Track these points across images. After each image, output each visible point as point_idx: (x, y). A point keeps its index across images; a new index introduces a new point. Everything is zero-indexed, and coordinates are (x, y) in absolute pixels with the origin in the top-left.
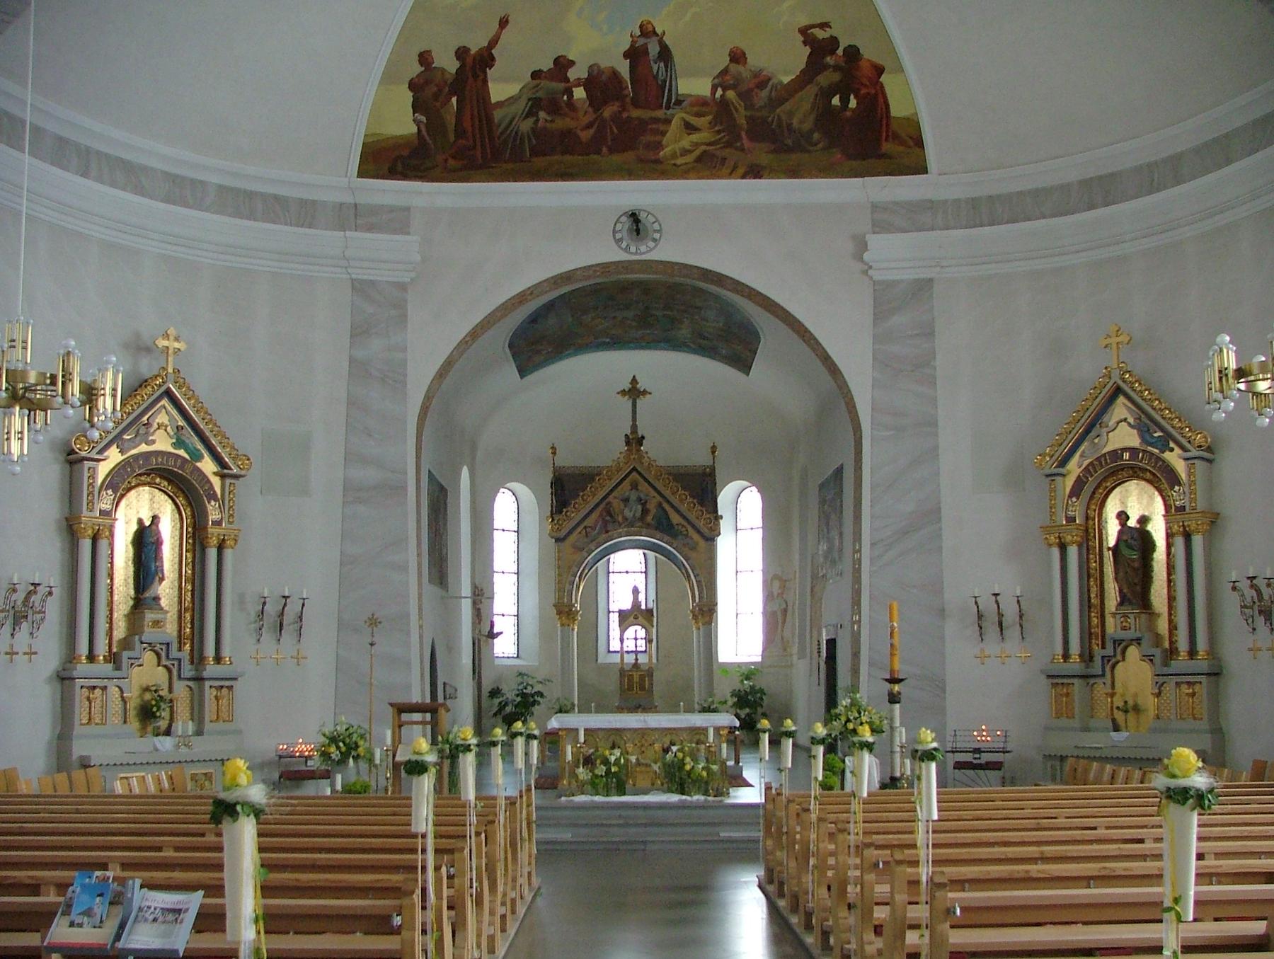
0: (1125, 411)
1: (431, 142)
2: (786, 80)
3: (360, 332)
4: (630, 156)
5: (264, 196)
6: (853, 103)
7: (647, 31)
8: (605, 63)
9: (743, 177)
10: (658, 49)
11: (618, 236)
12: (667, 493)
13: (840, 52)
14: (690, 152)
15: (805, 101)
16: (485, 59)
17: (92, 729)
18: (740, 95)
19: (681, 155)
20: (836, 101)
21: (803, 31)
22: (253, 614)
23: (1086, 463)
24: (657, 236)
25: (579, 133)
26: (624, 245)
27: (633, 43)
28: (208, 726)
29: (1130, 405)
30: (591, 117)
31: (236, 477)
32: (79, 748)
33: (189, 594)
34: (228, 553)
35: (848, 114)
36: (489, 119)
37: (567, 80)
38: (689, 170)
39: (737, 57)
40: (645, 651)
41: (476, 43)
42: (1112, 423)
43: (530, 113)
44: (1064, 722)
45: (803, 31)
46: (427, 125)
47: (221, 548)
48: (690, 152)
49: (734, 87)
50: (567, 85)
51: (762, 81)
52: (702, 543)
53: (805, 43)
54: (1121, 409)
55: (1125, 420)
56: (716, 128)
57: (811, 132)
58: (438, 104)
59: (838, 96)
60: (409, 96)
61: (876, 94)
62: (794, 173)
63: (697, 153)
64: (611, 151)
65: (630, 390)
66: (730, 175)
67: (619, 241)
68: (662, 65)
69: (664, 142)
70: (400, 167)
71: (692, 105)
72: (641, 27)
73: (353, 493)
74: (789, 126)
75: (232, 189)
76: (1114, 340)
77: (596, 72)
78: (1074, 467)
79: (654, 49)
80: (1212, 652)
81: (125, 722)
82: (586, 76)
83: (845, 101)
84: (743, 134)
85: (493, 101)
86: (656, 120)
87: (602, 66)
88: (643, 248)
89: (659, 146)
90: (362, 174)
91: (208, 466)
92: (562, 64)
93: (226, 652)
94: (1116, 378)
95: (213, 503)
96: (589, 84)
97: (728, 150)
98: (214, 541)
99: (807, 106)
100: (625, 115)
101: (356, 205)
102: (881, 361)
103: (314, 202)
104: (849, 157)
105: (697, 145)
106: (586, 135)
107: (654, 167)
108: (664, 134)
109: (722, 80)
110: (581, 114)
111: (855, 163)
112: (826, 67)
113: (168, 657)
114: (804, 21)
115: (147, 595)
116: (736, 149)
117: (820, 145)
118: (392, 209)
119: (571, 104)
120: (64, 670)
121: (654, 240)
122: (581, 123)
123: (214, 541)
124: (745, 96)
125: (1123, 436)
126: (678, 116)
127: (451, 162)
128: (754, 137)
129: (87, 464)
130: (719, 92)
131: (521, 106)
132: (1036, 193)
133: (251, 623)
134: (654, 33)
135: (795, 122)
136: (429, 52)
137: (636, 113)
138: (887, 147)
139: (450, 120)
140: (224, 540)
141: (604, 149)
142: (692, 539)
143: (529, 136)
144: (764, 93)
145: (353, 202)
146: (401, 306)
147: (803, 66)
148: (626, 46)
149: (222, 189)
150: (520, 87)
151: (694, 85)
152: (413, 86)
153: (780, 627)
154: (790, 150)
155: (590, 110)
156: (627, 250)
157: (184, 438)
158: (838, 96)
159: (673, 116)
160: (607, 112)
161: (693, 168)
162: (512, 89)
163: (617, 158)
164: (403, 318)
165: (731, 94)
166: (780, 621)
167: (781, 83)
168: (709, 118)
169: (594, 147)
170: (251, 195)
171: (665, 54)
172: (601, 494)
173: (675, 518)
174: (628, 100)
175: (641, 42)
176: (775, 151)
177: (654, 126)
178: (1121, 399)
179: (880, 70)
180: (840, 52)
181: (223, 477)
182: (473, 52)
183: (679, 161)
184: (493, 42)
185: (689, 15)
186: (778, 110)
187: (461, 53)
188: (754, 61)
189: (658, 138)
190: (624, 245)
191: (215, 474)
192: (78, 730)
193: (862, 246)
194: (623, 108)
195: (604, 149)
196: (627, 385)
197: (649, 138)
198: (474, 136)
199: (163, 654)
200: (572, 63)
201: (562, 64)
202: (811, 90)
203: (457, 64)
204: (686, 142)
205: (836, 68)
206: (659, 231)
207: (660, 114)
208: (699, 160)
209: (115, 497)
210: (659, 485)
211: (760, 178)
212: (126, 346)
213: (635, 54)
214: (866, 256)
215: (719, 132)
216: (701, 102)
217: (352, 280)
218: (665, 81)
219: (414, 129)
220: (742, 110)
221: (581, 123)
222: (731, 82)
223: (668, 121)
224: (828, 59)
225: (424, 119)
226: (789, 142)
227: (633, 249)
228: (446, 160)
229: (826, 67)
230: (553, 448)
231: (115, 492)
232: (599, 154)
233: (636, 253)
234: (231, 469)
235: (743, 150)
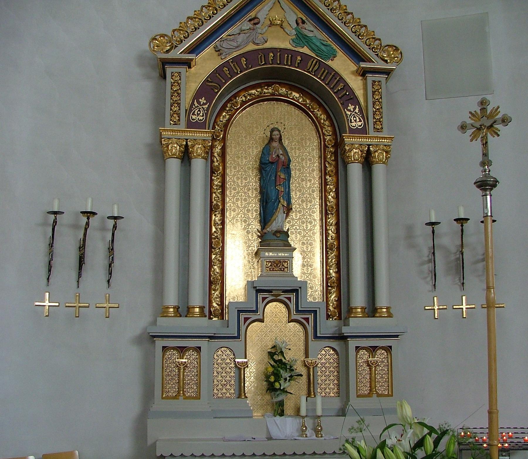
17: (180, 404)
22: (426, 252)
28: (354, 402)
33: (333, 228)
34: (379, 170)
81: (239, 396)
93: (382, 301)
95: (351, 107)
98: (355, 153)
123: (355, 153)
133: (422, 264)
140: (369, 152)
157: (306, 32)
181: (363, 73)
209: (209, 106)
231: (209, 100)
234: (370, 61)
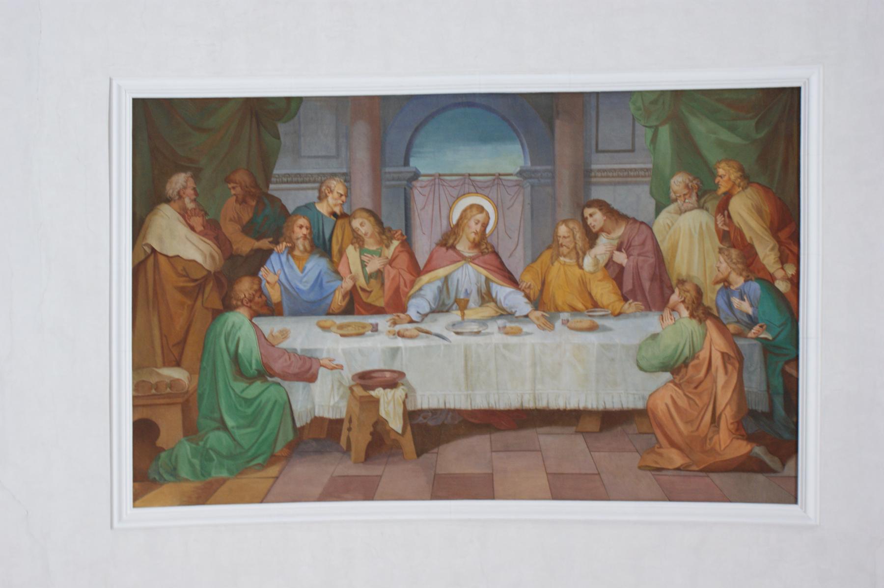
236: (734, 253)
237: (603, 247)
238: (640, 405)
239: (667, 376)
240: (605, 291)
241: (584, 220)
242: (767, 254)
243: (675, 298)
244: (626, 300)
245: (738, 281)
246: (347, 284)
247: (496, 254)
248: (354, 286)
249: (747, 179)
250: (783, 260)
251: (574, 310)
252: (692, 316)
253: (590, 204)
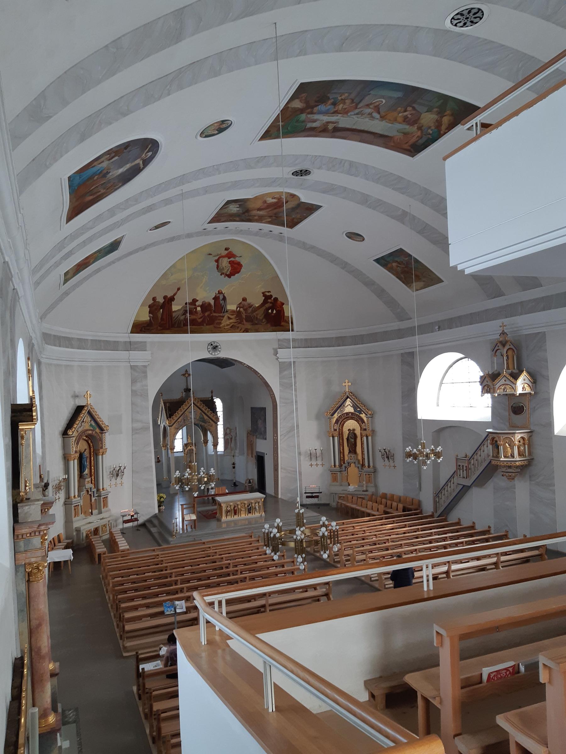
0: (350, 403)
1: (153, 322)
2: (257, 306)
3: (134, 381)
4: (212, 326)
5: (104, 341)
6: (275, 312)
7: (220, 292)
8: (207, 301)
9: (243, 332)
10: (223, 297)
11: (209, 350)
12: (204, 410)
13: (272, 299)
14: (229, 325)
15: (261, 311)
16: (172, 299)
18: (244, 310)
19: (227, 326)
20: (270, 311)
21: (263, 293)
23: (339, 415)
24: (220, 350)
25: (198, 320)
26: (211, 352)
27: (215, 296)
29: (350, 401)
30: (201, 315)
31: (105, 433)
32: (76, 525)
35: (273, 314)
36: (171, 316)
37: (196, 305)
38: (228, 331)
39: (244, 300)
40: (182, 451)
41: (169, 295)
42: (346, 406)
43: (184, 314)
44: (335, 483)
45: (263, 293)
46: (153, 318)
47: (102, 455)
48: (229, 325)
49: (242, 307)
50: (196, 307)
51: (250, 306)
52: (214, 424)
53: (263, 296)
54: (348, 402)
55: (350, 405)
56: (237, 318)
57: (262, 319)
58: (156, 312)
59: (270, 310)
60: (148, 309)
61: (281, 310)
62: (257, 331)
63: (231, 325)
64: (207, 325)
65: (185, 374)
66: (239, 332)
67: (209, 352)
68: (223, 301)
69: (222, 322)
70: (143, 330)
71: (231, 312)
72: (218, 291)
73: (135, 431)
74: (257, 318)
75: (94, 340)
76: (347, 384)
77: (204, 303)
78: (336, 416)
79: (221, 297)
80: (374, 467)
82: (201, 304)
83: (272, 311)
84: (244, 320)
85: (173, 310)
86: (220, 316)
87: (206, 301)
88: (216, 354)
89: (220, 323)
90: (132, 332)
91: (98, 430)
92: (195, 301)
94: (347, 394)
96: (202, 306)
97: (240, 324)
99: (262, 313)
100: (211, 315)
101: (130, 342)
102: (281, 384)
103: (118, 342)
104: (272, 326)
105: (231, 323)
106: (200, 320)
107: (218, 329)
108: (222, 320)
109: (239, 306)
110: (199, 314)
111: (274, 328)
112: (268, 302)
113: (91, 491)
114: (264, 291)
115: (84, 473)
116: (242, 324)
117: (265, 323)
118: (141, 342)
119: (196, 312)
120: (65, 501)
121: (219, 351)
122: (198, 317)
124: (245, 310)
125: (349, 408)
126: (226, 315)
127: (159, 328)
128: (247, 321)
129: (71, 438)
130: (239, 309)
131: (181, 312)
132: (323, 339)
134: (222, 293)
135: (258, 317)
136: (155, 297)
137: (215, 314)
138: (283, 323)
139: (160, 316)
141: (205, 324)
142: (211, 423)
143: (183, 322)
144: (251, 309)
145: (129, 341)
146: (145, 372)
147: (262, 302)
148: (214, 296)
149: (92, 340)
150: (181, 306)
151: (231, 307)
152: (150, 306)
153: (230, 444)
154: (256, 324)
155: (202, 313)
156: (211, 354)
158: (270, 310)
159: (225, 315)
160: (206, 314)
161: (230, 329)
162: (179, 307)
163: (208, 327)
164: (146, 377)
165: (242, 309)
166: (230, 442)
167: (255, 306)
168: (235, 316)
169: (201, 324)
170: (100, 341)
171: (224, 299)
172: (183, 411)
173: (206, 417)
174: (213, 311)
175: (218, 295)
176: (252, 325)
177: (219, 318)
178: (348, 399)
179: (283, 304)
180: (272, 299)
182: (168, 297)
183: (225, 328)
184: (175, 294)
185: (233, 288)
186: (254, 314)
187: (165, 297)
188: (249, 301)
189: (220, 321)
190: (211, 352)
191: (100, 433)
192: (74, 519)
193: (276, 353)
194: (211, 313)
195: (205, 324)
196: (184, 373)
197: (218, 321)
198: (166, 320)
199: (89, 490)
200: (198, 301)
201: (195, 301)
202: (264, 308)
203: (164, 300)
204: (228, 322)
205: (271, 303)
206: (220, 348)
207: (221, 314)
208: (231, 327)
210: (201, 407)
211: (248, 332)
212: (72, 397)
213: (216, 299)
214: (277, 355)
215: (237, 320)
216: (233, 311)
217: (131, 366)
218: (223, 306)
219: (149, 319)
220: (244, 314)
221: (198, 317)
222: (242, 306)
223: (223, 317)
224: (269, 300)
225: (152, 315)
226: (256, 322)
227: (213, 354)
228: (157, 327)
229: (268, 302)
230: (161, 394)
232: (203, 325)
233: (214, 355)
235: (243, 324)
236: (437, 124)
237: (405, 114)
238: (392, 136)
239: (403, 134)
240: (400, 119)
241: (407, 108)
242: (443, 127)
243: (416, 125)
244: (404, 122)
245: (433, 128)
246: (336, 109)
247: (379, 109)
248: (337, 110)
249: (452, 115)
250: (446, 129)
251: (390, 120)
252: (417, 129)
253: (410, 106)
